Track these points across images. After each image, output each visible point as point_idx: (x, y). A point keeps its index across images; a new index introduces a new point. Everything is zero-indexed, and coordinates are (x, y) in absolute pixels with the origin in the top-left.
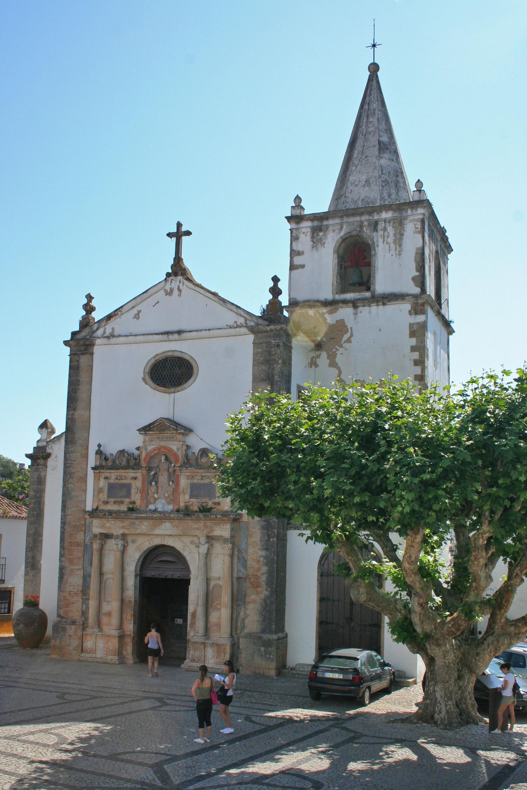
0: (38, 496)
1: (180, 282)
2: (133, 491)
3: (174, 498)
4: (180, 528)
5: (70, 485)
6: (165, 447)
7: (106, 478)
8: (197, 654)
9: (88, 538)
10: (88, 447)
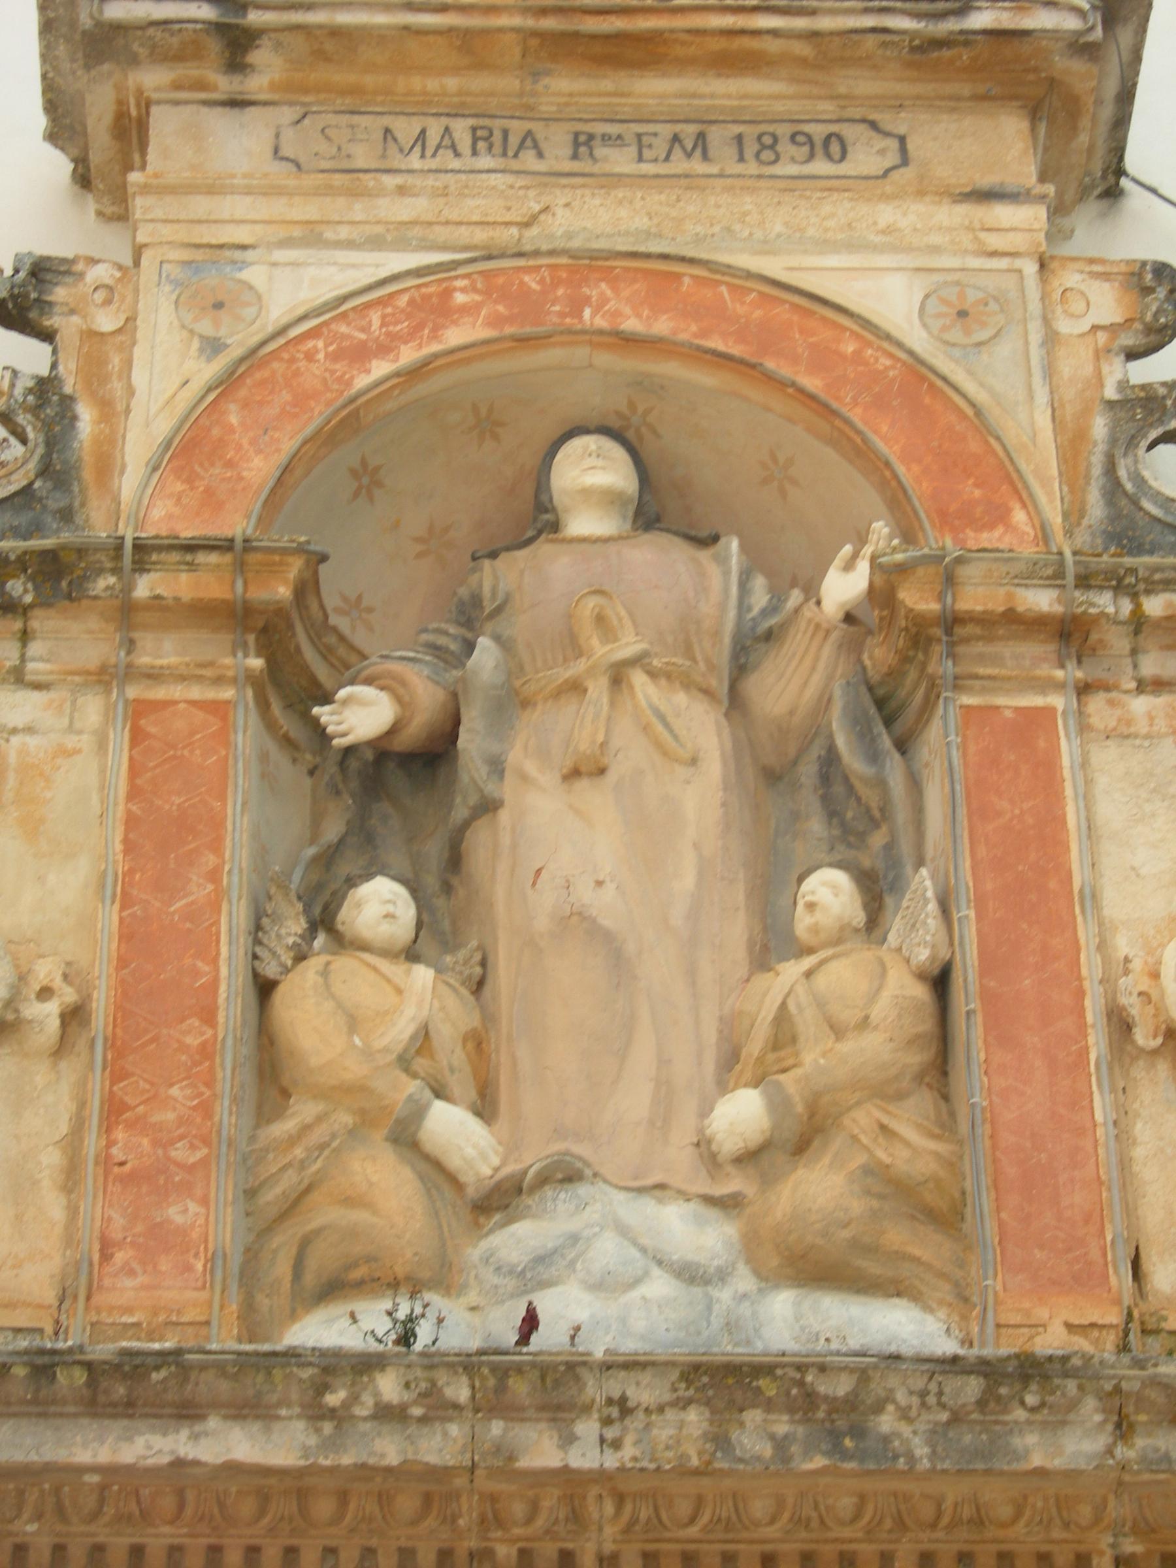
6: (657, 270)
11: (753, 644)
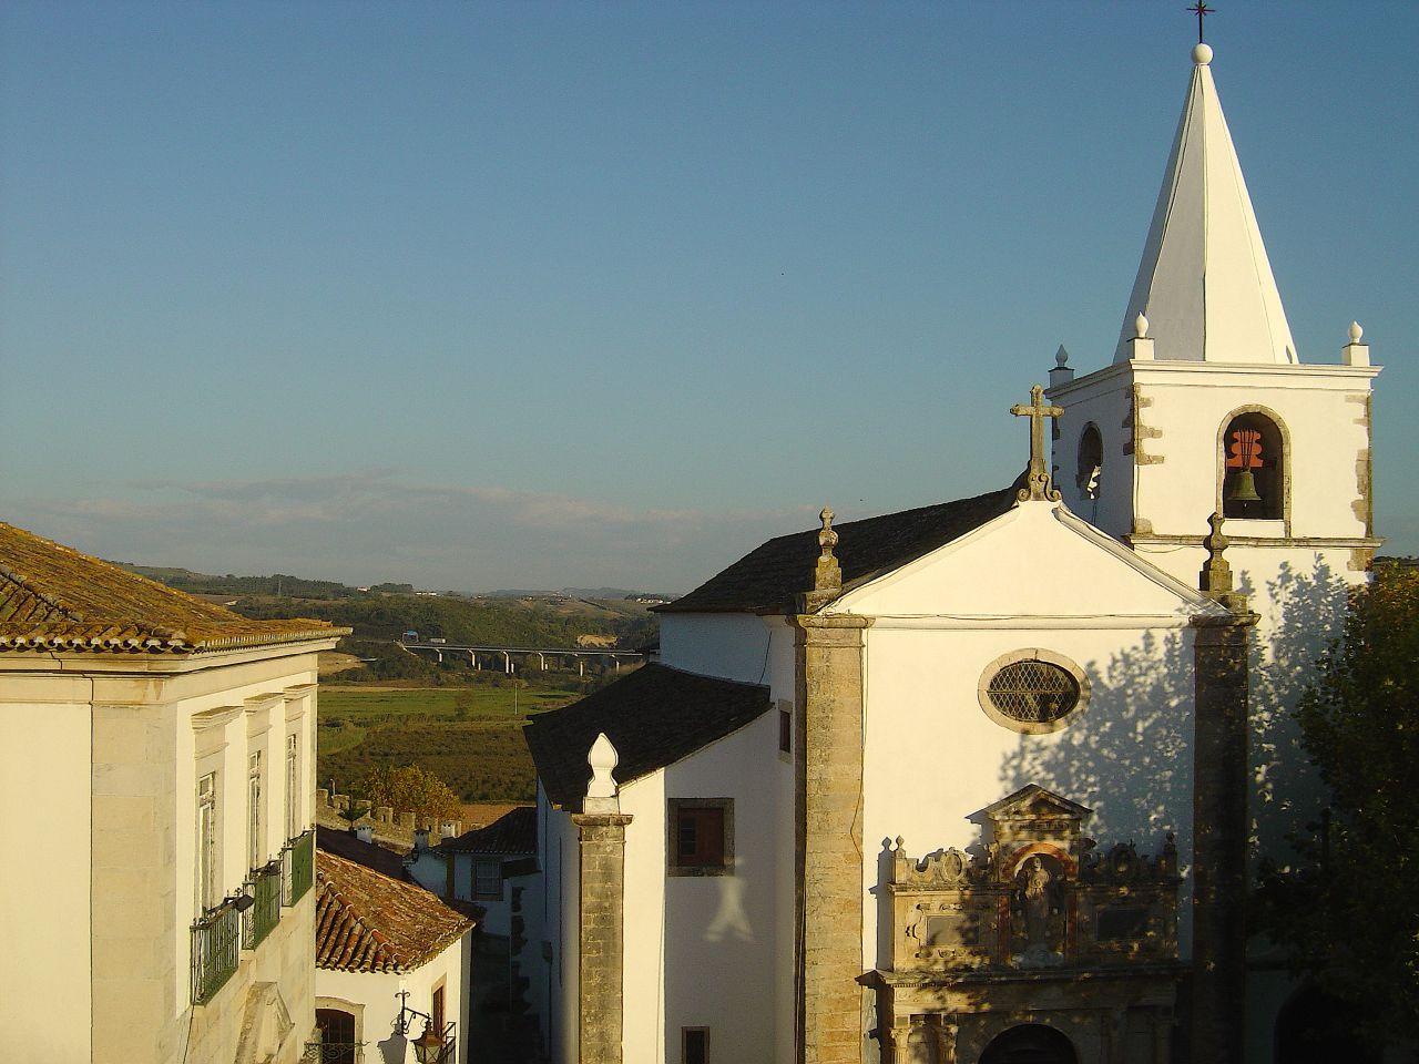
0: (607, 905)
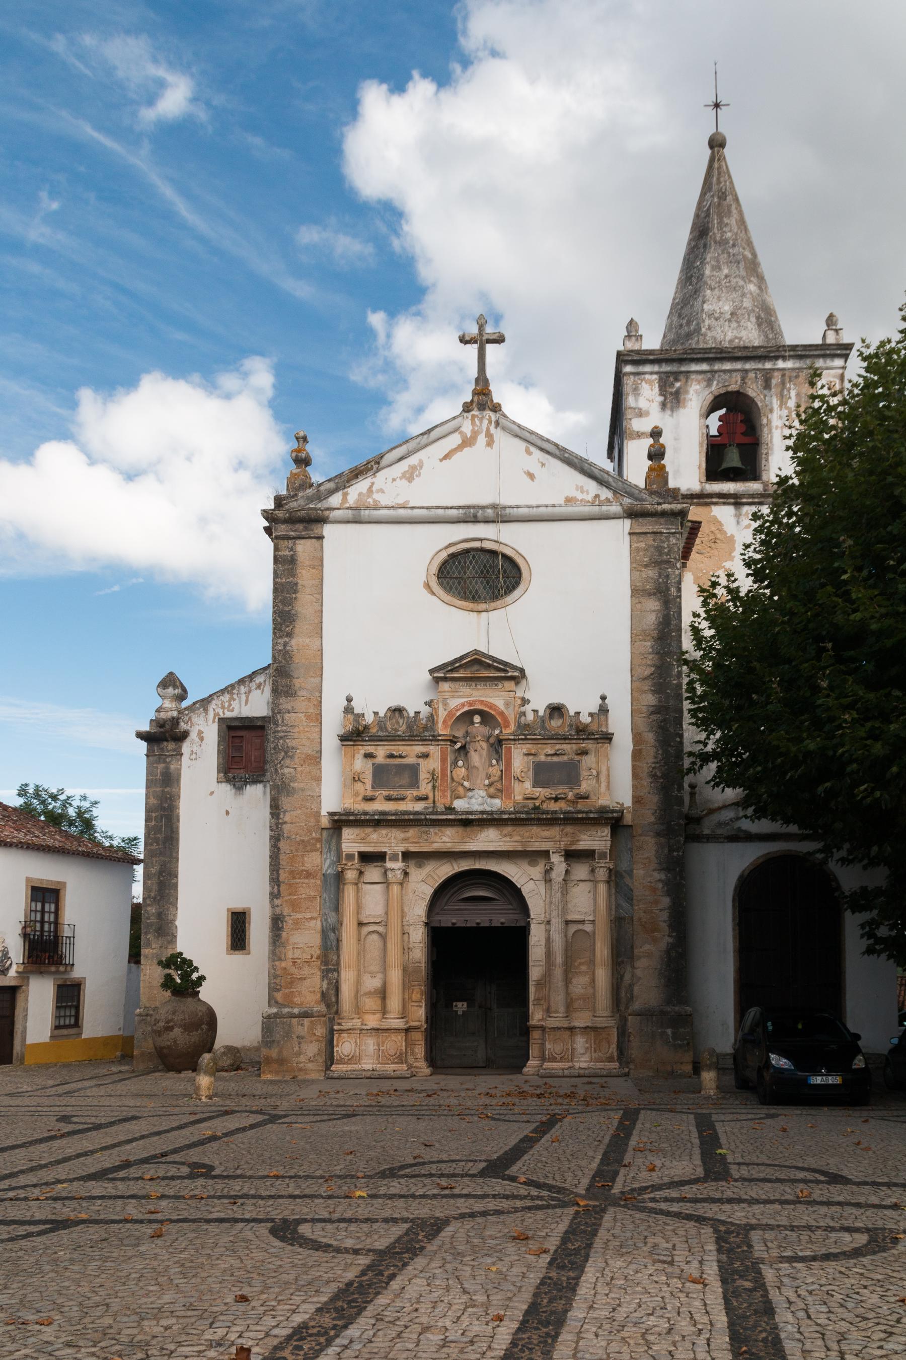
1: (490, 422)
2: (423, 775)
3: (499, 788)
4: (517, 838)
5: (286, 771)
6: (482, 702)
7: (369, 756)
8: (558, 1048)
9: (328, 862)
10: (321, 702)
11: (489, 737)
